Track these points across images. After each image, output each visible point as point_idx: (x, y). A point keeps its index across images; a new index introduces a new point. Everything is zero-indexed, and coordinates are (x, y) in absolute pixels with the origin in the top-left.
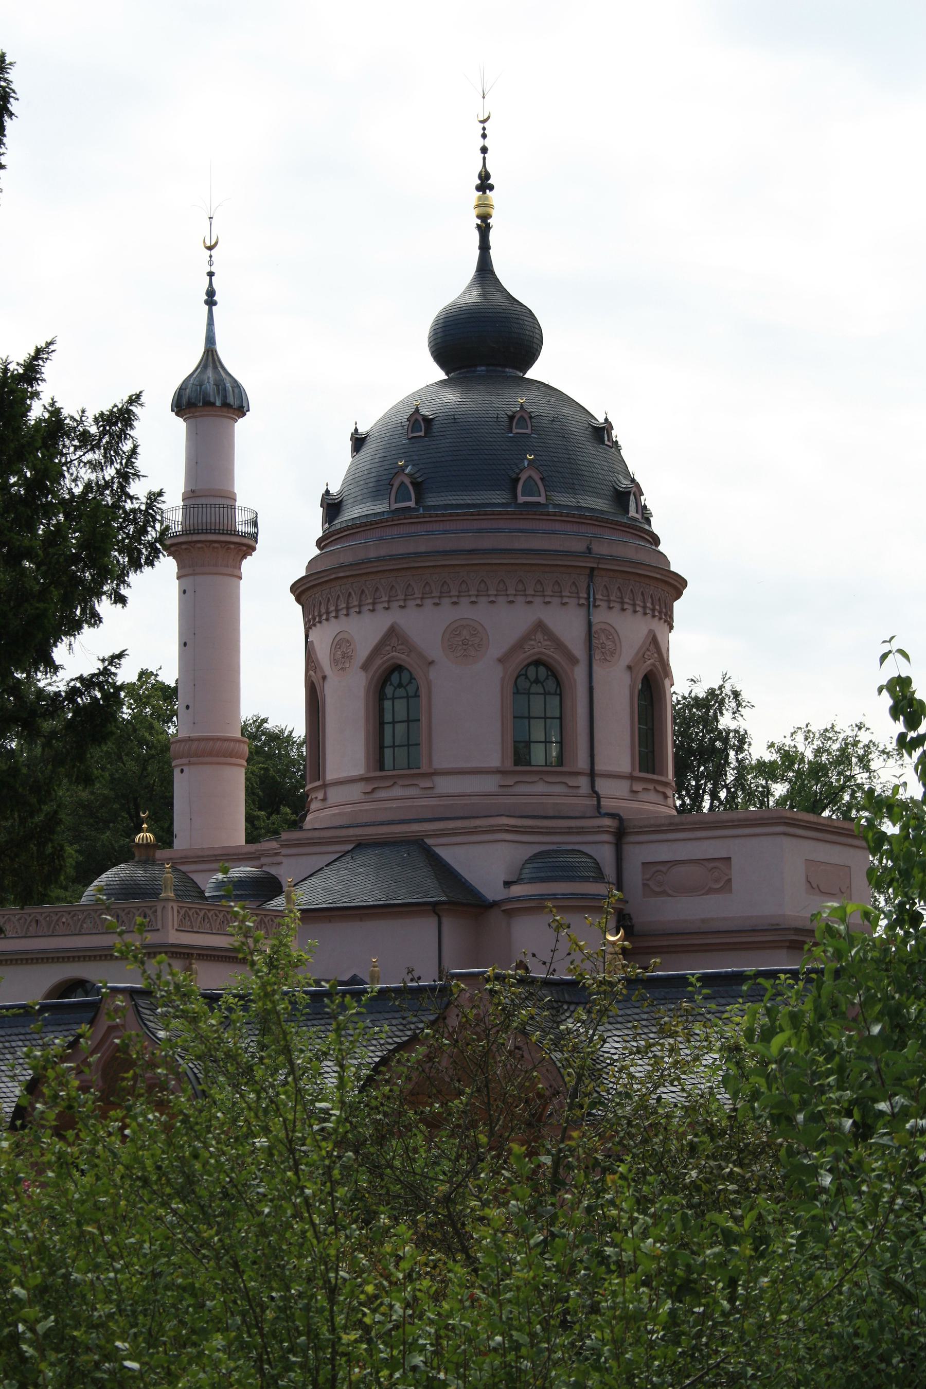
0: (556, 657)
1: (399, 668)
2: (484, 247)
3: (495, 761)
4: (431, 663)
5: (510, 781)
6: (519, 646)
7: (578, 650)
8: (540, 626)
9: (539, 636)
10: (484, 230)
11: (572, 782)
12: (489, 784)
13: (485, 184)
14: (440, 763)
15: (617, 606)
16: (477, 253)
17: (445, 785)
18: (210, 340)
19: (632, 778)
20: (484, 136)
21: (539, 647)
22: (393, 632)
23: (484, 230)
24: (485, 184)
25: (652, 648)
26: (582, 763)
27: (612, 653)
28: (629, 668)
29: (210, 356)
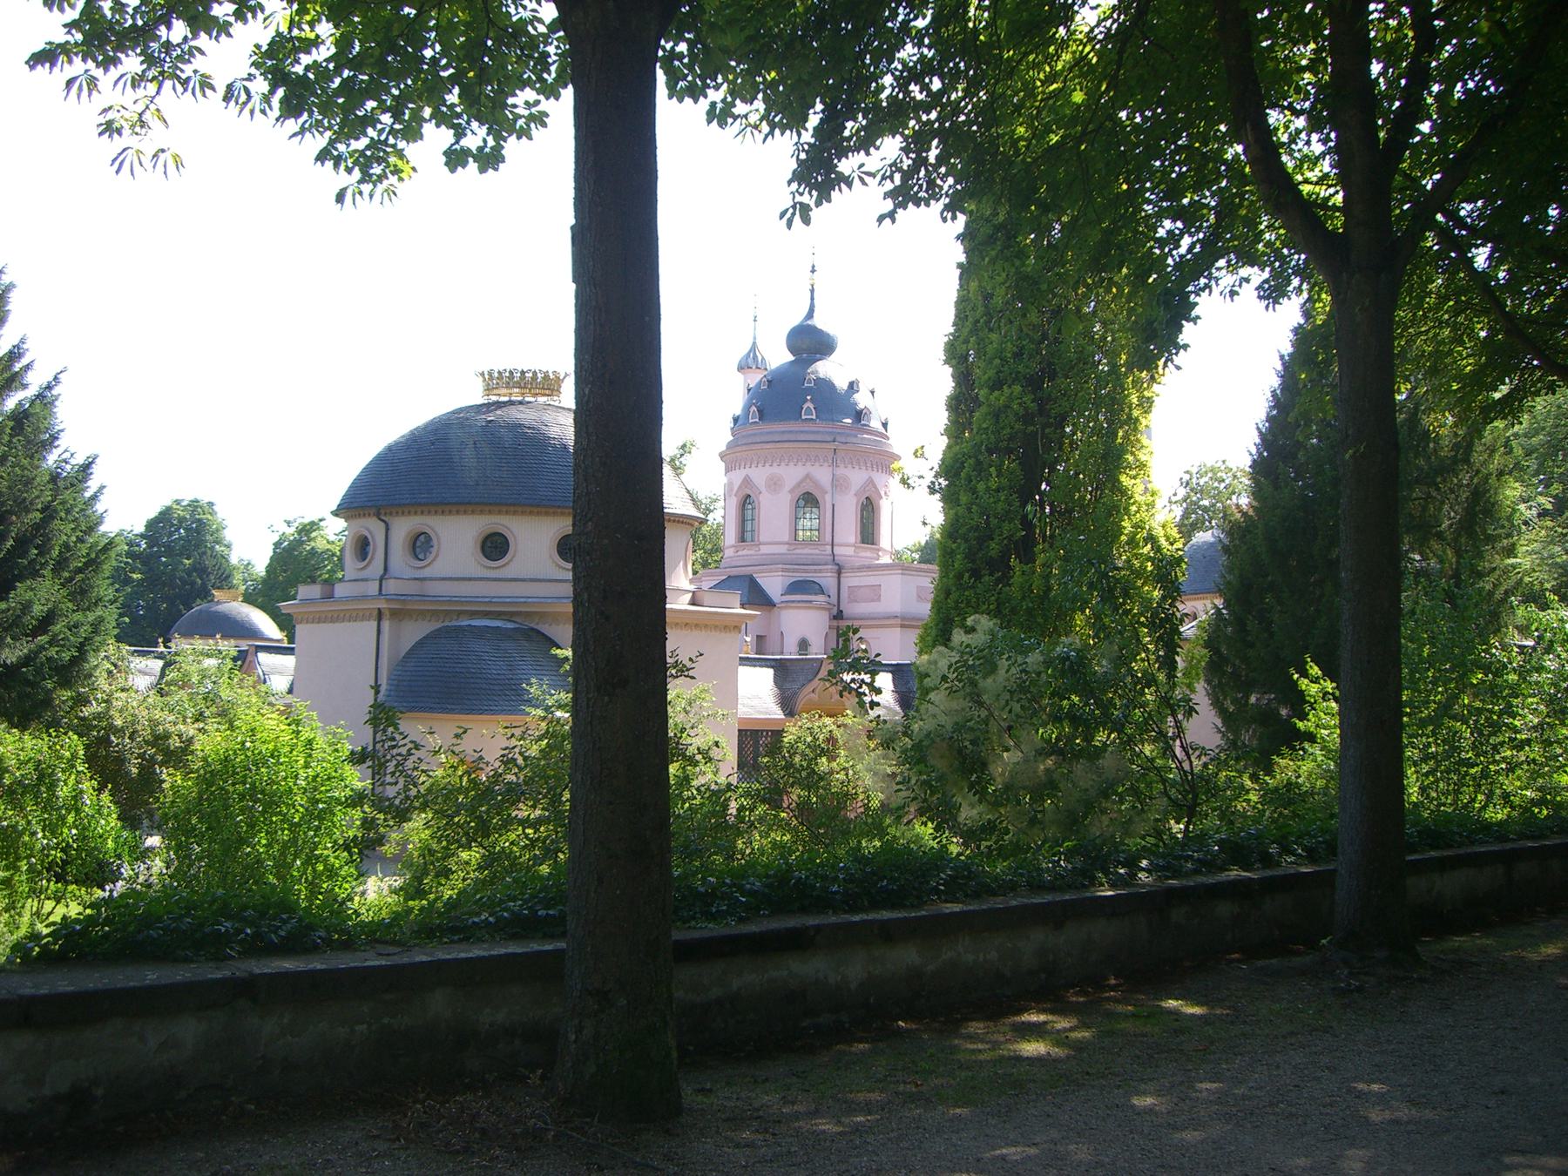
1: (749, 496)
2: (812, 299)
5: (792, 547)
6: (799, 485)
7: (828, 486)
11: (822, 548)
12: (783, 549)
15: (850, 466)
16: (809, 301)
17: (764, 549)
18: (755, 338)
22: (747, 481)
23: (812, 291)
24: (813, 271)
26: (828, 538)
27: (846, 488)
29: (754, 347)
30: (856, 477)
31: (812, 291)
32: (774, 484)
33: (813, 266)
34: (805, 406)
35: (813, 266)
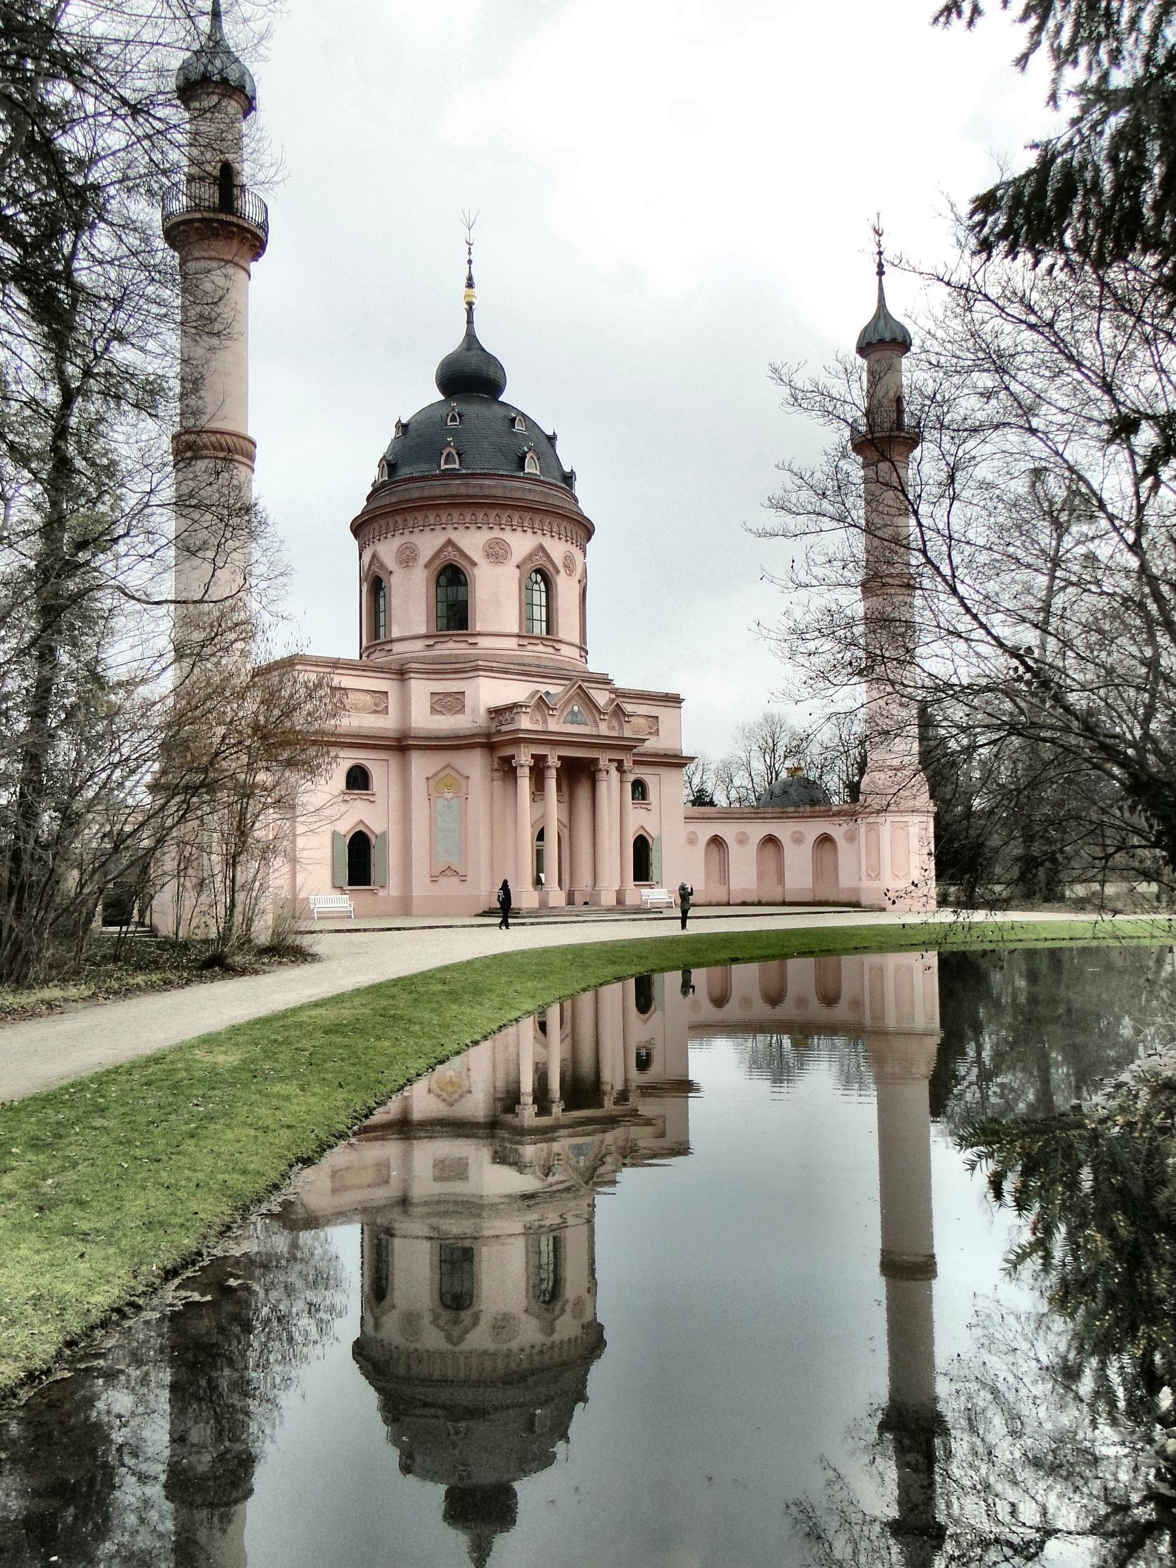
0: (462, 563)
2: (470, 322)
3: (423, 630)
4: (391, 572)
8: (450, 542)
9: (450, 549)
10: (470, 311)
13: (470, 285)
14: (395, 634)
19: (518, 636)
20: (470, 253)
21: (450, 555)
22: (374, 556)
23: (470, 311)
24: (470, 285)
25: (541, 554)
28: (518, 567)
32: (407, 558)
33: (470, 278)
34: (445, 453)
35: (470, 278)
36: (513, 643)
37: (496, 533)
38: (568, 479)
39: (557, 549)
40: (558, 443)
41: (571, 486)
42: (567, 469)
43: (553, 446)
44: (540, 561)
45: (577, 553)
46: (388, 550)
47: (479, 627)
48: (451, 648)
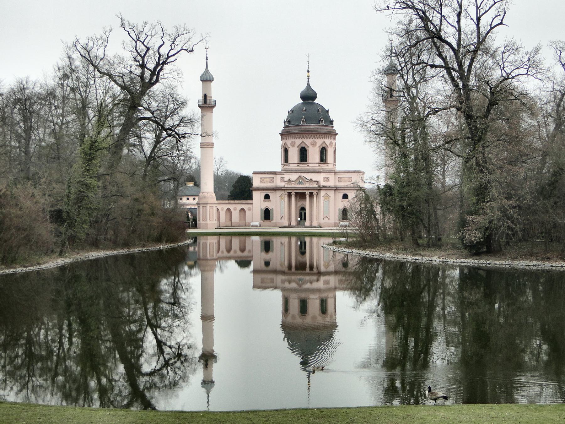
2: (308, 81)
3: (297, 162)
8: (303, 142)
13: (308, 72)
21: (303, 145)
23: (308, 79)
24: (308, 72)
30: (320, 142)
31: (308, 79)
32: (293, 144)
36: (317, 165)
37: (314, 140)
38: (331, 122)
39: (328, 141)
40: (329, 112)
41: (332, 124)
42: (332, 119)
43: (328, 113)
44: (324, 145)
45: (333, 141)
46: (289, 142)
47: (309, 162)
48: (303, 166)
